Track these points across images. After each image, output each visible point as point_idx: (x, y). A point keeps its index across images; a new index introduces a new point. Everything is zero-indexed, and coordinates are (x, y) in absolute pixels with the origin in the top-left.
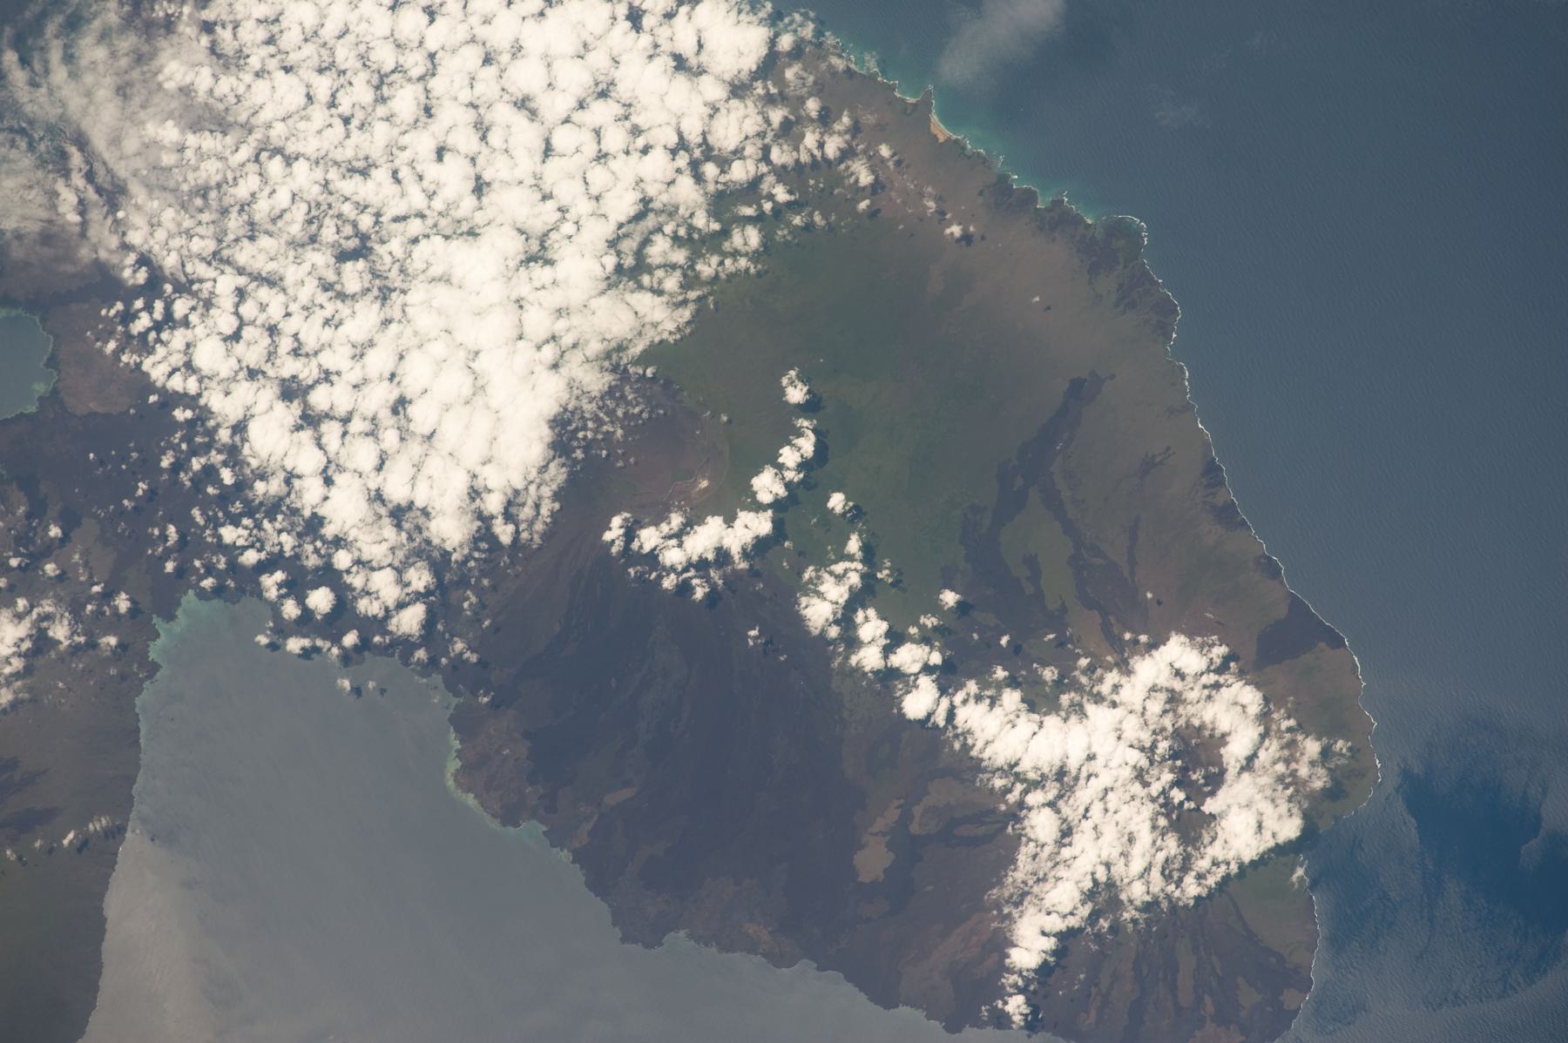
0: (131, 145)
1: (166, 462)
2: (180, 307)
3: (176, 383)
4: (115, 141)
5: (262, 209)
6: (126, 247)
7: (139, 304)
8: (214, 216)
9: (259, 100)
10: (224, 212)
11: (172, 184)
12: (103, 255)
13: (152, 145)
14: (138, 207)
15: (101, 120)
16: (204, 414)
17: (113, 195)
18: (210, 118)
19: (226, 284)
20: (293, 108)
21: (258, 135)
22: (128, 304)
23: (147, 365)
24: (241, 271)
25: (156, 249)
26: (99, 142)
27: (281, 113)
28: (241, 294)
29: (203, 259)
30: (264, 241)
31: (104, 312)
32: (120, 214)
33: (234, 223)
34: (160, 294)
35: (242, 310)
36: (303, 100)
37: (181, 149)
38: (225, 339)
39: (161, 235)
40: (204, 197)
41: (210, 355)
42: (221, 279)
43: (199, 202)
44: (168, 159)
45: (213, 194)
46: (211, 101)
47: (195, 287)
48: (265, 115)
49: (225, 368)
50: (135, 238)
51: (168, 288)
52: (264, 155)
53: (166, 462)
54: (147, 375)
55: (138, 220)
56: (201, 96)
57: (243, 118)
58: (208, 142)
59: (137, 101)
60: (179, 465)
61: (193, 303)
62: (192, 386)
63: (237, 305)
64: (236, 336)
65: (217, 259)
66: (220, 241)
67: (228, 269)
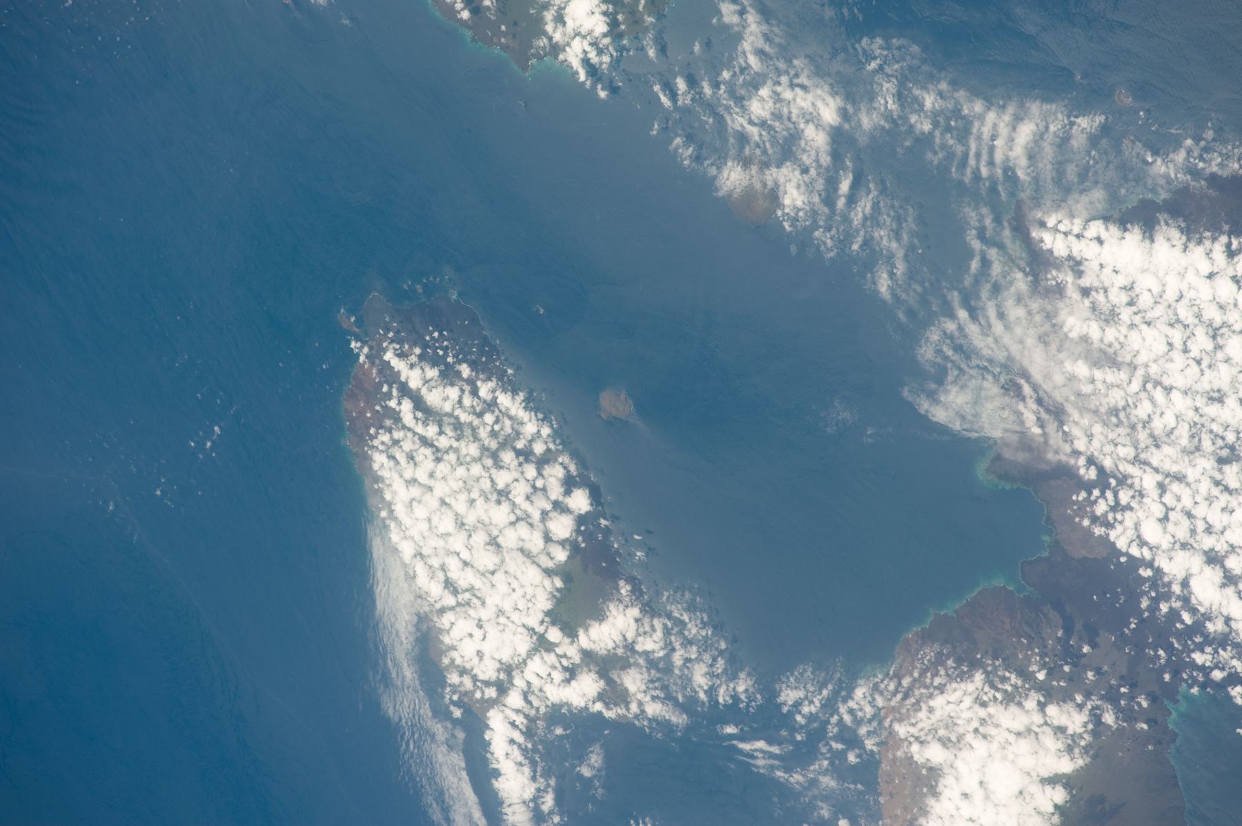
0: (1059, 379)
1: (1145, 604)
2: (1124, 497)
3: (1135, 551)
4: (1048, 376)
5: (1158, 425)
6: (1076, 453)
7: (1096, 492)
8: (1128, 430)
9: (1136, 346)
10: (1133, 427)
11: (1092, 407)
12: (1063, 458)
13: (1072, 378)
14: (1077, 424)
15: (1036, 361)
16: (1159, 572)
17: (1058, 413)
18: (1107, 358)
19: (1149, 481)
20: (1160, 353)
21: (1140, 372)
22: (1090, 493)
23: (1113, 535)
24: (1157, 470)
25: (1096, 454)
26: (1037, 376)
27: (1153, 357)
28: (1162, 488)
29: (1129, 462)
30: (1167, 450)
31: (1074, 498)
32: (1066, 428)
33: (1142, 436)
34: (1108, 486)
35: (1164, 500)
36: (1166, 348)
37: (1093, 381)
38: (1160, 520)
39: (1096, 444)
40: (1117, 416)
41: (1152, 532)
42: (1145, 477)
43: (1114, 420)
44: (1087, 389)
45: (1122, 415)
46: (1103, 346)
47: (1129, 482)
48: (1142, 359)
49: (1165, 542)
50: (1080, 445)
51: (1113, 482)
52: (1149, 386)
53: (1145, 604)
54: (1114, 543)
55: (1076, 432)
56: (1096, 344)
57: (1128, 359)
58: (1111, 376)
59: (1053, 347)
60: (1154, 608)
61: (1131, 493)
62: (1147, 554)
63: (1161, 496)
64: (1165, 519)
65: (1136, 461)
66: (1136, 448)
67: (1148, 469)
